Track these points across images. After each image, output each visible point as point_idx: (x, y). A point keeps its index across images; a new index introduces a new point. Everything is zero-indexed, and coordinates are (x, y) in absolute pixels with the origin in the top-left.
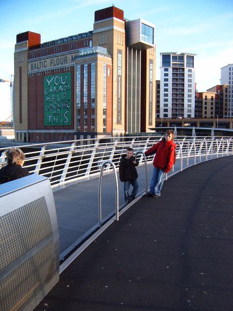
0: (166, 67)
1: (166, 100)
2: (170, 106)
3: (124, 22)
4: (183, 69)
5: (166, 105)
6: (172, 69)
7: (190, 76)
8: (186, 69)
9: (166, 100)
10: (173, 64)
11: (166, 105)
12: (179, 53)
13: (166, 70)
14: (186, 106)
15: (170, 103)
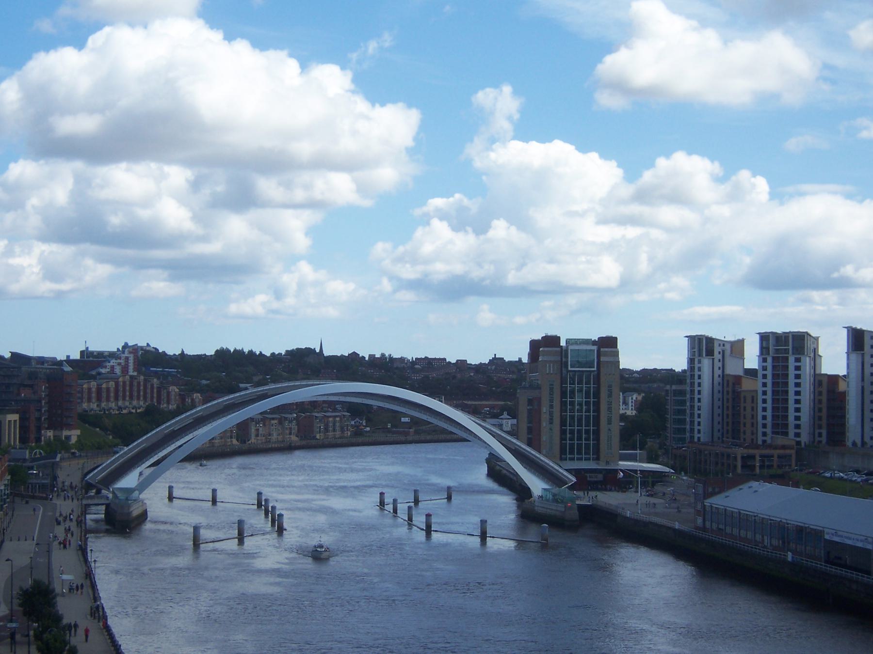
0: (764, 357)
1: (764, 409)
2: (769, 418)
3: (558, 349)
4: (787, 359)
5: (764, 418)
6: (771, 358)
7: (798, 368)
8: (791, 359)
9: (764, 409)
10: (788, 346)
11: (764, 418)
12: (779, 330)
13: (765, 360)
14: (791, 418)
15: (769, 413)
